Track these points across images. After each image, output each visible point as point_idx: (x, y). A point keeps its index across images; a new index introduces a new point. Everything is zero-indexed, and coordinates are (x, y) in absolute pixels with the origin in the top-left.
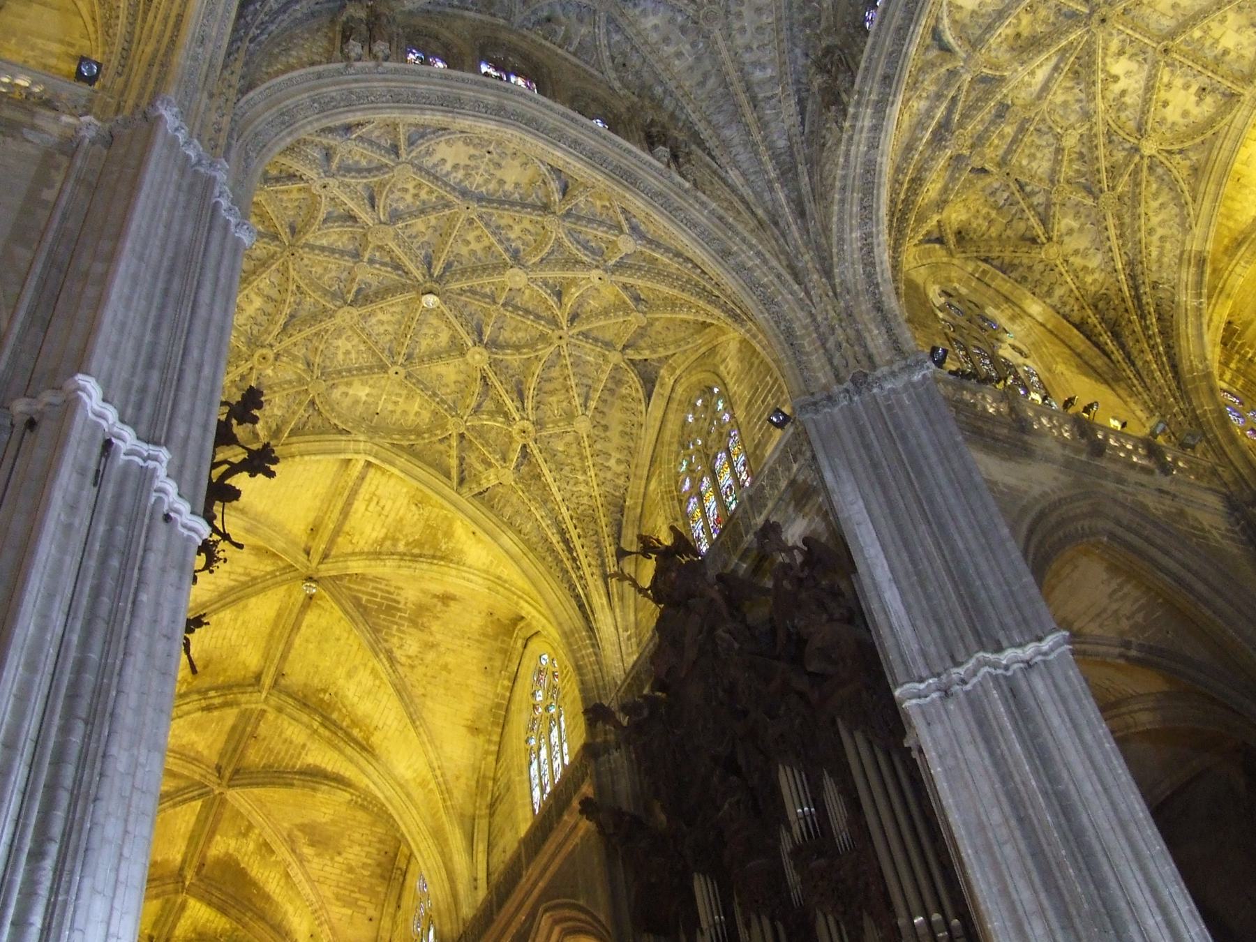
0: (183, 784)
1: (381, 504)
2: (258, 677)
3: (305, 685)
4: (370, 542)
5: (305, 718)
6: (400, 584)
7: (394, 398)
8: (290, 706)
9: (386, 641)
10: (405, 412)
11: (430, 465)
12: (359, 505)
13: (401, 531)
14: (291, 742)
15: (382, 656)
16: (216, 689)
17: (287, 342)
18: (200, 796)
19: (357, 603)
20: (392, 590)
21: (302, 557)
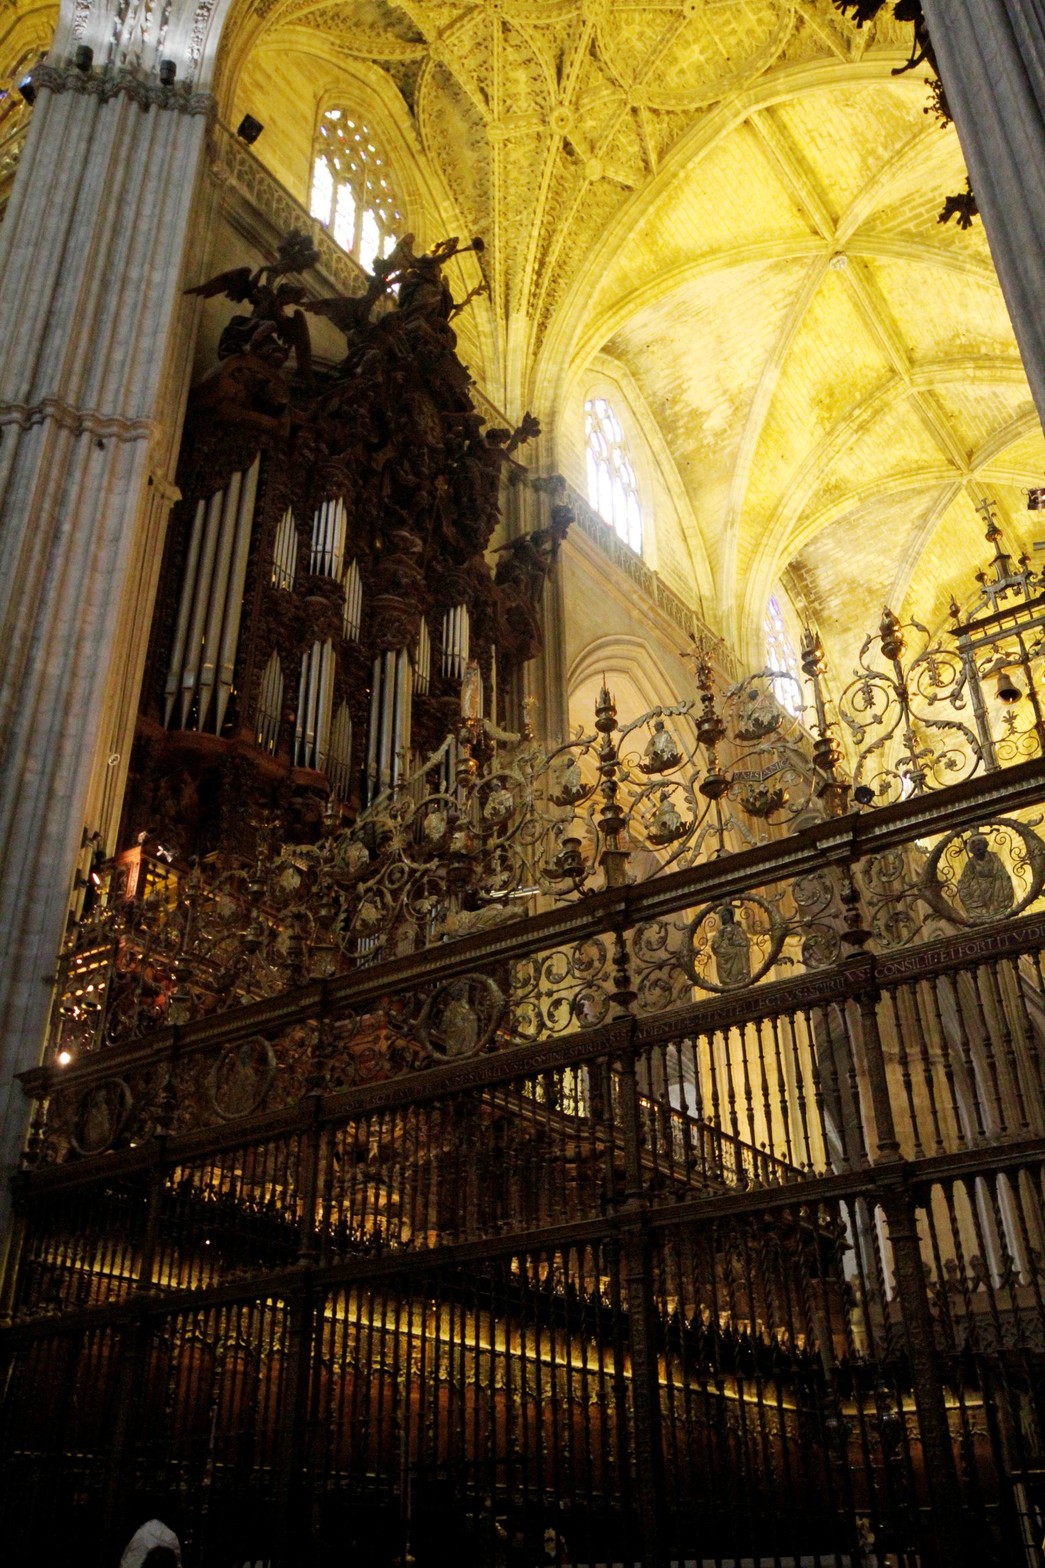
0: (935, 494)
1: (825, 134)
2: (892, 370)
3: (937, 343)
4: (857, 174)
5: (957, 373)
6: (933, 184)
7: (727, 29)
8: (938, 372)
9: (965, 248)
10: (750, 32)
11: (812, 59)
12: (811, 153)
13: (867, 141)
14: (983, 399)
15: (968, 266)
16: (859, 406)
17: (570, 84)
18: (955, 494)
19: (908, 236)
20: (930, 196)
21: (815, 241)
